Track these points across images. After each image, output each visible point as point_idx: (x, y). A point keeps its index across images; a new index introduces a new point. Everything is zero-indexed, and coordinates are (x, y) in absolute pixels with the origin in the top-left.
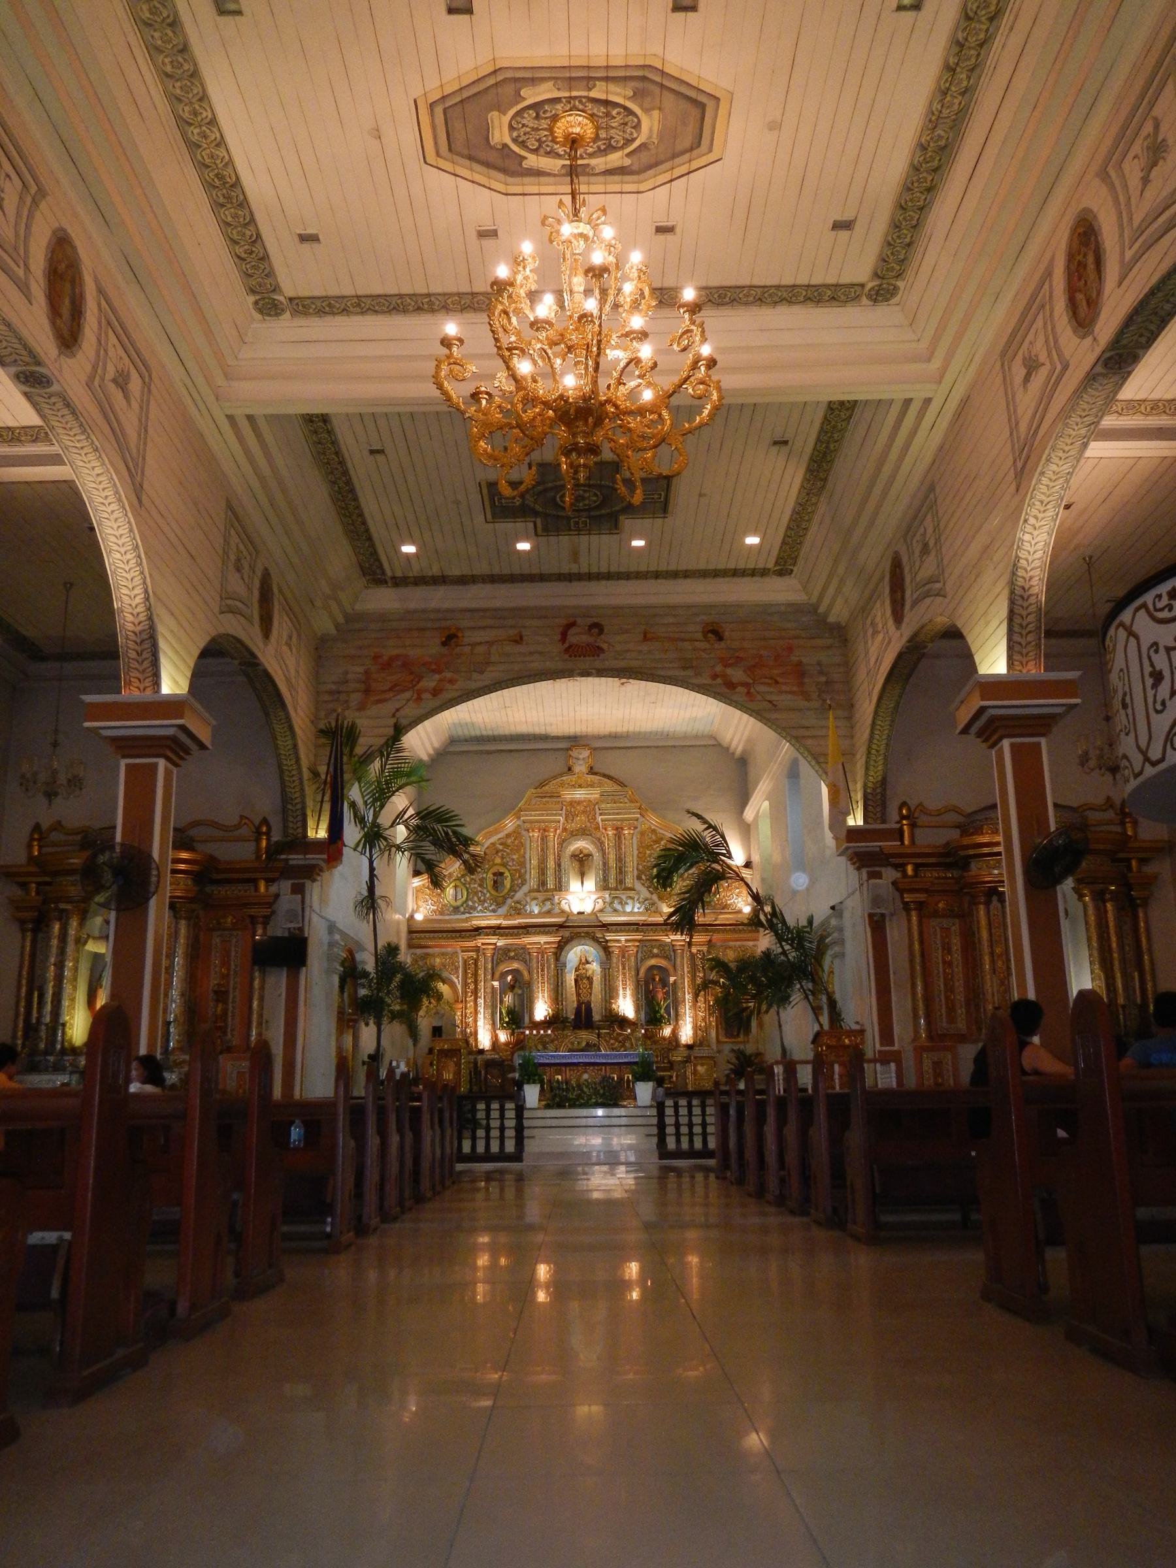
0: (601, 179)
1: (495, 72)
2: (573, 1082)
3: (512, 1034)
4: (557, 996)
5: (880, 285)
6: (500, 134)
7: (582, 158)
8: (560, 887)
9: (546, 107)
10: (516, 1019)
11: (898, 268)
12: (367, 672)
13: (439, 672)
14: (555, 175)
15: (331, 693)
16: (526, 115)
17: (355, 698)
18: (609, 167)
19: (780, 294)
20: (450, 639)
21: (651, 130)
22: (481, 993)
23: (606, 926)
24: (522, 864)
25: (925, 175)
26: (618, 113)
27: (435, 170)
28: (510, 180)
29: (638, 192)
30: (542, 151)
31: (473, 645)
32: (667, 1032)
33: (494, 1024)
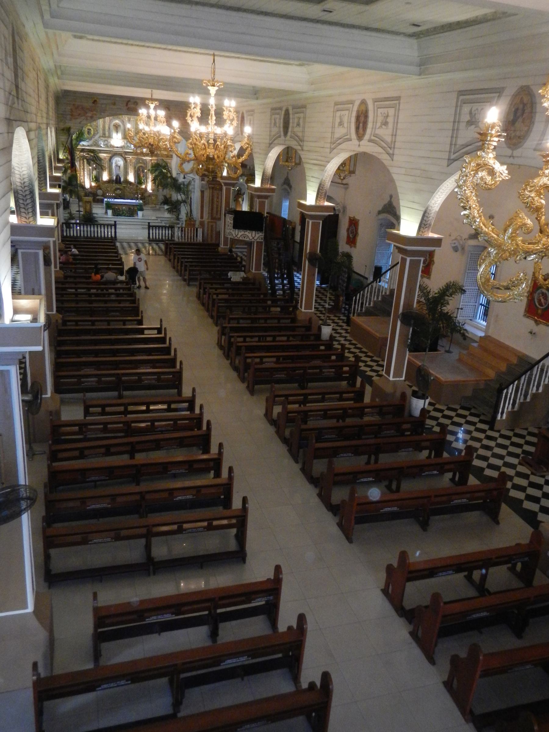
2: (121, 209)
3: (96, 184)
4: (110, 174)
8: (110, 137)
10: (97, 179)
12: (71, 109)
13: (92, 111)
15: (62, 114)
17: (68, 117)
20: (95, 102)
22: (86, 170)
23: (126, 153)
24: (97, 127)
31: (102, 104)
32: (143, 187)
33: (90, 179)
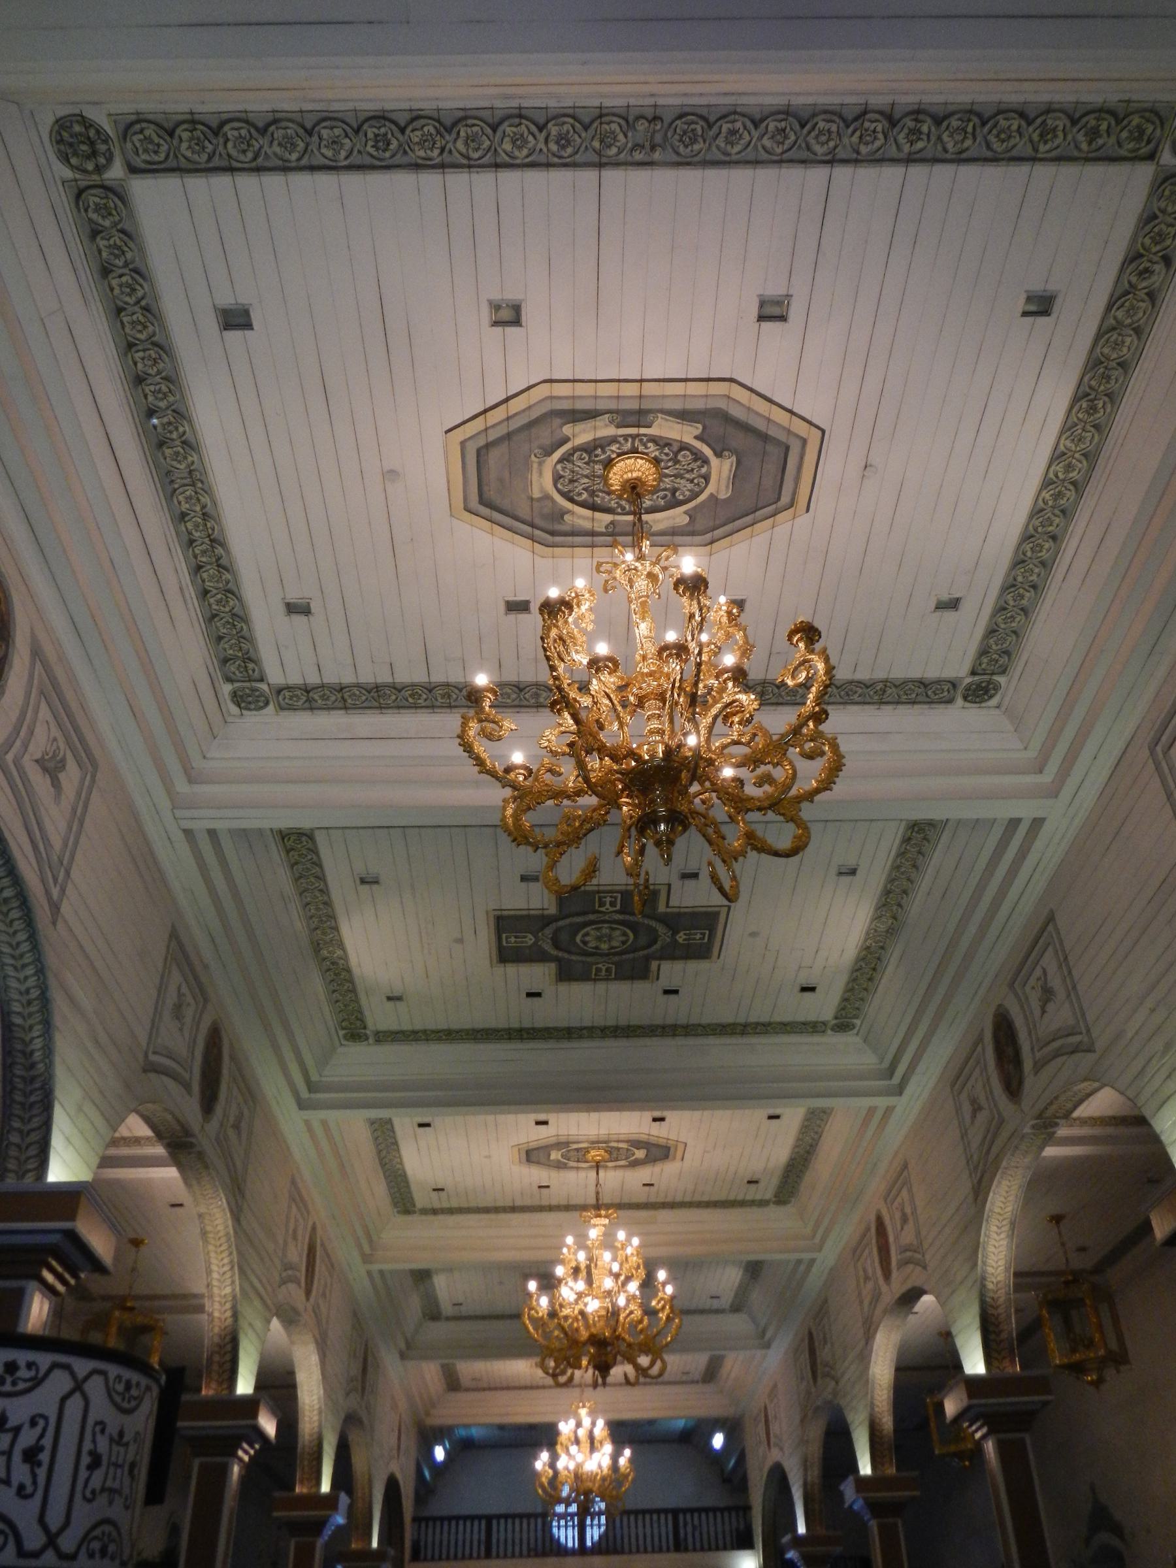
0: (601, 405)
1: (712, 543)
5: (99, 169)
6: (721, 469)
7: (626, 437)
9: (662, 502)
11: (94, 216)
14: (662, 411)
16: (687, 493)
18: (590, 424)
19: (277, 149)
21: (540, 473)
25: (163, 404)
26: (580, 494)
27: (815, 421)
28: (722, 404)
29: (551, 381)
30: (675, 448)
